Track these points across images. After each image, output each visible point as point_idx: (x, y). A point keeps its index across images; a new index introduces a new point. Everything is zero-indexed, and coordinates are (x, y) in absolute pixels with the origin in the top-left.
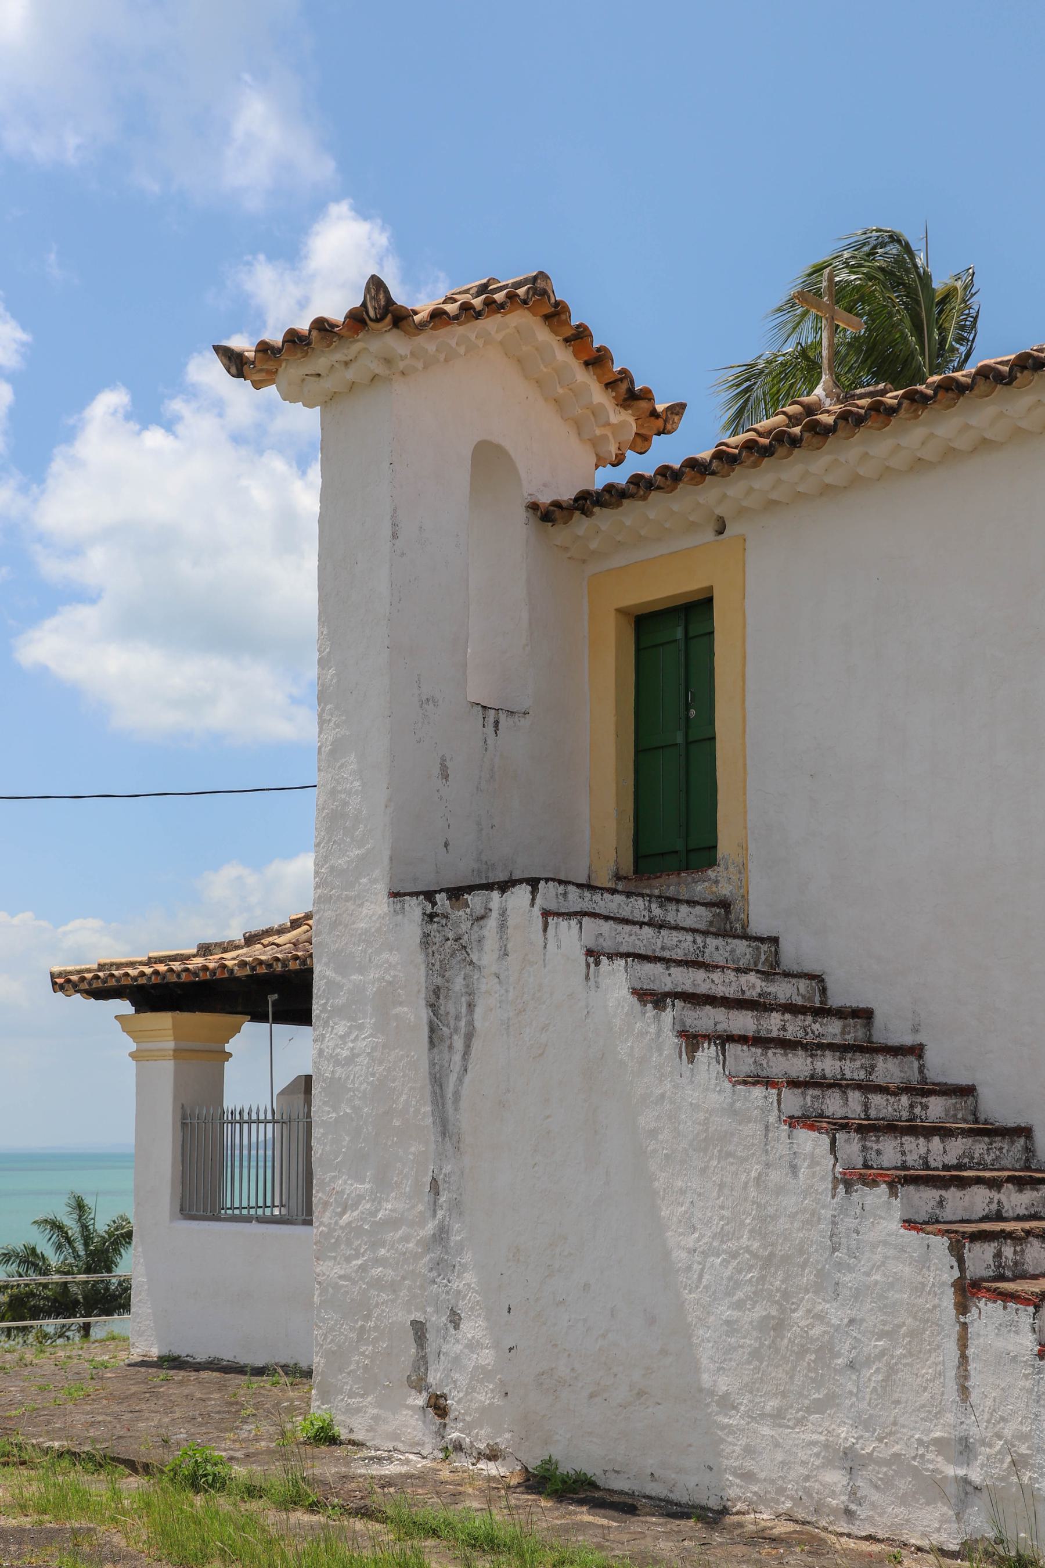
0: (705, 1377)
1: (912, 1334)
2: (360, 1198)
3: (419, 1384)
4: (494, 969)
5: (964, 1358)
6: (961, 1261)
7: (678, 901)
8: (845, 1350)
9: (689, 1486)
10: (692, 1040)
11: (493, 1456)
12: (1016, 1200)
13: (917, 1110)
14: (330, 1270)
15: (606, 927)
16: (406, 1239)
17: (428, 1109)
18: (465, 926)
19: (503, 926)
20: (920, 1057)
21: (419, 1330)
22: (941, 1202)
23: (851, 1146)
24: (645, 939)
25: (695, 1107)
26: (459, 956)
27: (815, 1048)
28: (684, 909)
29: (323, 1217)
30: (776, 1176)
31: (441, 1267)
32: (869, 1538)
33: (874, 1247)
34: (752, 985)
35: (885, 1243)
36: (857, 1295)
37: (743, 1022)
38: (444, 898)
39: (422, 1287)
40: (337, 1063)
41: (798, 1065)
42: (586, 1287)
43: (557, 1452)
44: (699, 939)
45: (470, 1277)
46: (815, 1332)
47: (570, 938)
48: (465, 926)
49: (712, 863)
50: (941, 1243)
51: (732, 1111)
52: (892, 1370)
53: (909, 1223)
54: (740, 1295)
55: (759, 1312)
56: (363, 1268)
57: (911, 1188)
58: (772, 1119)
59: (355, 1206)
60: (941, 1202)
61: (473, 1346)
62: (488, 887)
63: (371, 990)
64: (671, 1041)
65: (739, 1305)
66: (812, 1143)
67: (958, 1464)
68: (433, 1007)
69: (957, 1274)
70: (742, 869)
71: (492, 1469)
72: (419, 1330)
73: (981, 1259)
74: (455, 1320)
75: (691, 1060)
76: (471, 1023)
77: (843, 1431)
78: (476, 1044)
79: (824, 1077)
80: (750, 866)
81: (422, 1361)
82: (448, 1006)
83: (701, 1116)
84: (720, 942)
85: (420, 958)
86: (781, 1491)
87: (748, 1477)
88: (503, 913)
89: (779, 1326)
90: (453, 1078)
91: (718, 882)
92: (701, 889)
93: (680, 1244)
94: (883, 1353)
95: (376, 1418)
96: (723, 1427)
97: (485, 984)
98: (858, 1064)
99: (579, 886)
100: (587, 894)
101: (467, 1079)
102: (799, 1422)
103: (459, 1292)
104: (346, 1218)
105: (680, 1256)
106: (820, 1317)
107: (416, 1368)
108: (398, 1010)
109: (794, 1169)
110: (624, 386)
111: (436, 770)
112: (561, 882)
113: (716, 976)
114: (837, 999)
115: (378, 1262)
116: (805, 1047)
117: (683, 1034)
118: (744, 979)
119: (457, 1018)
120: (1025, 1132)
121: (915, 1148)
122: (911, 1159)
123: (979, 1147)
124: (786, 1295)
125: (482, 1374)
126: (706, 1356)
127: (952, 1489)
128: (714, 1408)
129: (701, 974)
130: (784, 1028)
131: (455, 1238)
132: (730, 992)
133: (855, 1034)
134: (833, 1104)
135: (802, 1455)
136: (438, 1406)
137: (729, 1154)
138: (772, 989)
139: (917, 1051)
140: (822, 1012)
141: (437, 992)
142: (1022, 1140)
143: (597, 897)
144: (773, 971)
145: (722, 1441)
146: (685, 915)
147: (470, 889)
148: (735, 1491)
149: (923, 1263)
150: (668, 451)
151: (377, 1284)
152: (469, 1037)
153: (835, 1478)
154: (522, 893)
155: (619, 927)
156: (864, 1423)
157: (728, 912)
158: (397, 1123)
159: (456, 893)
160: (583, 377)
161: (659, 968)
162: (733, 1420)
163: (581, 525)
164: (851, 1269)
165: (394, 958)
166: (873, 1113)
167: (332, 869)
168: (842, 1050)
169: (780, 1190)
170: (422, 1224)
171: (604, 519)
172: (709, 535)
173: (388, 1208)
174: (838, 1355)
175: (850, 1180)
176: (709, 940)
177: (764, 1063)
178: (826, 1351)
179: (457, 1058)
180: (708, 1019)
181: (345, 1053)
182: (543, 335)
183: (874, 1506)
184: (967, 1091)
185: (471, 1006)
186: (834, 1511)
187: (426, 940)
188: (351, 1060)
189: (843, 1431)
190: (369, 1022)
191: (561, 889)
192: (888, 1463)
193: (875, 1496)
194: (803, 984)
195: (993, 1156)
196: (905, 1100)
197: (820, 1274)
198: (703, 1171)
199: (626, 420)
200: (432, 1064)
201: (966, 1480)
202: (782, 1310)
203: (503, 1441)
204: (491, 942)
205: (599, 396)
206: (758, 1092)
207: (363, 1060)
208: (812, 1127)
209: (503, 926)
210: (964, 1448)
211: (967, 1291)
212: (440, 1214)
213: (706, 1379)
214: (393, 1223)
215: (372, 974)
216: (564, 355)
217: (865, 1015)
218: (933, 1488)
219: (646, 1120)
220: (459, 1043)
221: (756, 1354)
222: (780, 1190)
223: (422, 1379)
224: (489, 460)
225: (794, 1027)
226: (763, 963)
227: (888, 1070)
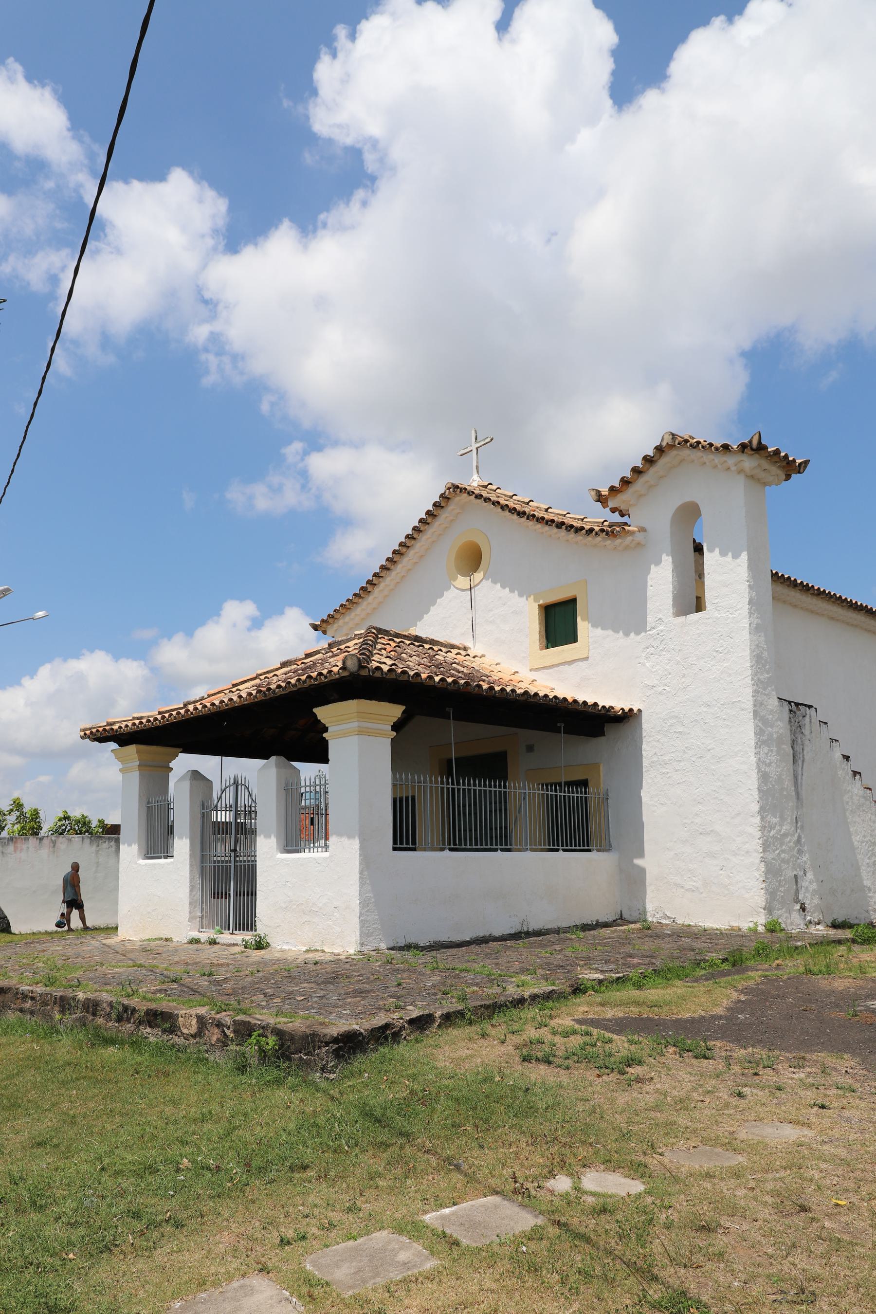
3: (797, 900)
11: (819, 924)
17: (793, 788)
31: (800, 852)
51: (864, 797)
56: (779, 854)
63: (775, 736)
65: (869, 858)
85: (789, 727)
93: (856, 839)
104: (772, 833)
108: (784, 746)
115: (783, 851)
136: (803, 909)
141: (793, 741)
152: (803, 761)
158: (785, 793)
159: (797, 704)
167: (759, 679)
173: (786, 828)
181: (768, 761)
187: (790, 721)
188: (770, 765)
204: (807, 726)
214: (785, 835)
215: (775, 730)
219: (846, 798)
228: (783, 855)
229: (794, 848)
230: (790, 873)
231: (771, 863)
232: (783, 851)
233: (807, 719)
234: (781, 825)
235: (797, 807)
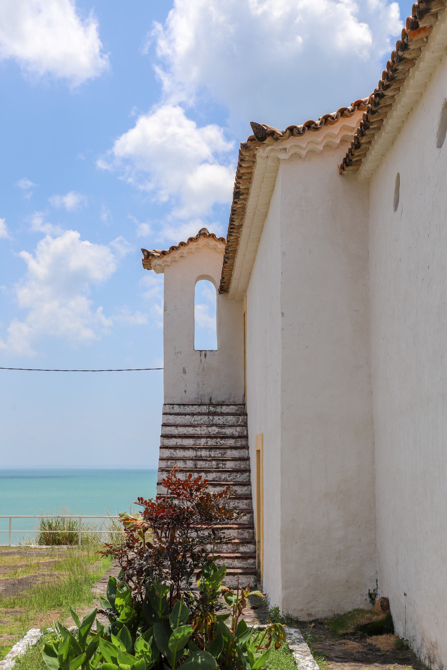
15: (171, 417)
20: (248, 449)
28: (224, 408)
44: (211, 417)
79: (201, 457)
98: (218, 452)
99: (178, 405)
100: (182, 407)
112: (171, 405)
113: (198, 429)
118: (210, 429)
129: (191, 429)
130: (207, 443)
138: (223, 431)
142: (248, 474)
143: (186, 407)
155: (176, 417)
161: (173, 428)
166: (199, 466)
176: (215, 417)
177: (175, 454)
191: (171, 406)
195: (231, 478)
196: (214, 463)
226: (241, 422)
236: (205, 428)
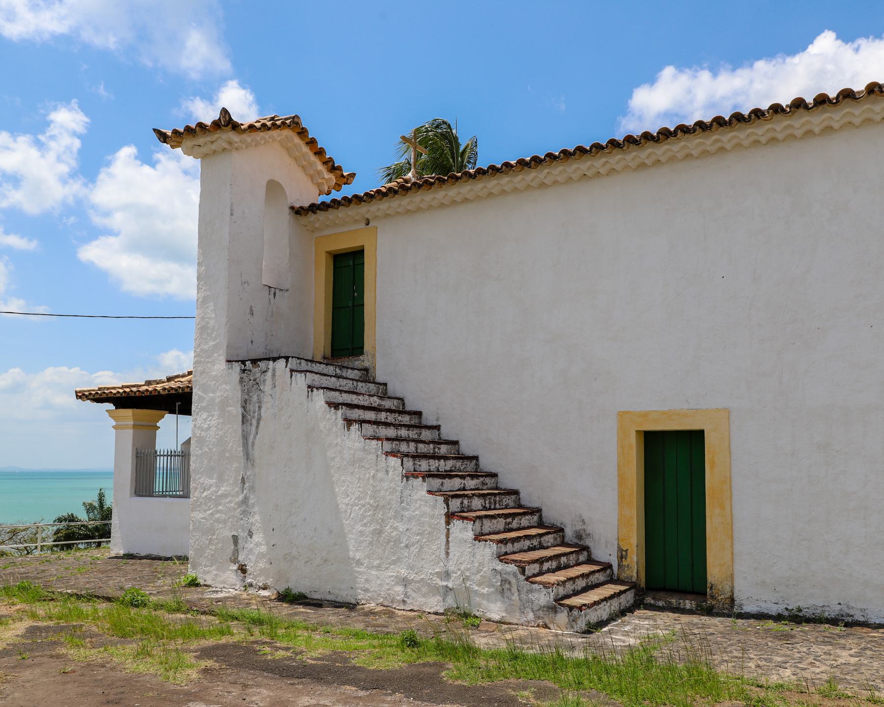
0: (351, 553)
1: (429, 533)
2: (211, 486)
3: (235, 560)
4: (270, 393)
5: (448, 541)
6: (448, 505)
7: (347, 368)
8: (405, 541)
9: (344, 595)
10: (349, 422)
11: (265, 588)
12: (471, 483)
13: (436, 450)
14: (198, 515)
15: (316, 377)
16: (230, 502)
18: (258, 375)
19: (274, 375)
20: (439, 430)
21: (235, 539)
22: (442, 484)
23: (409, 463)
24: (332, 382)
25: (349, 448)
26: (255, 387)
27: (397, 426)
28: (350, 371)
29: (195, 495)
30: (380, 475)
31: (245, 513)
32: (411, 610)
33: (416, 501)
34: (375, 401)
35: (420, 500)
36: (410, 520)
37: (370, 415)
38: (249, 364)
39: (237, 522)
40: (202, 430)
41: (391, 432)
42: (305, 519)
43: (291, 585)
45: (257, 517)
46: (393, 534)
47: (301, 381)
48: (258, 375)
49: (362, 353)
50: (441, 499)
51: (364, 450)
52: (422, 547)
53: (430, 492)
54: (365, 521)
55: (372, 527)
56: (212, 514)
57: (431, 479)
58: (379, 453)
59: (209, 489)
60: (442, 484)
61: (258, 545)
62: (268, 359)
63: (217, 400)
64: (341, 422)
65: (365, 525)
66: (394, 462)
67: (445, 581)
68: (244, 407)
69: (446, 510)
70: (374, 356)
71: (265, 593)
72: (235, 539)
73: (455, 504)
74: (251, 534)
75: (349, 429)
76: (259, 414)
77: (403, 571)
78: (262, 423)
80: (377, 355)
81: (236, 552)
82: (250, 407)
83: (352, 452)
84: (363, 384)
86: (379, 595)
87: (366, 590)
88: (274, 370)
89: (380, 532)
90: (252, 437)
91: (364, 361)
92: (357, 364)
93: (343, 502)
94: (418, 541)
95: (216, 575)
96: (357, 572)
97: (266, 399)
101: (258, 437)
102: (387, 569)
103: (252, 523)
105: (342, 507)
106: (396, 528)
107: (234, 554)
109: (387, 472)
110: (330, 164)
111: (248, 311)
112: (298, 358)
113: (361, 397)
114: (408, 408)
115: (218, 512)
116: (394, 425)
117: (345, 419)
118: (372, 399)
119: (254, 412)
120: (476, 458)
121: (434, 464)
122: (432, 468)
123: (459, 464)
124: (383, 520)
125: (262, 556)
126: (351, 545)
127: (441, 590)
128: (354, 565)
129: (354, 397)
131: (251, 501)
132: (366, 404)
133: (415, 421)
134: (404, 447)
135: (387, 581)
136: (243, 569)
137: (362, 467)
138: (383, 403)
139: (438, 428)
140: (401, 413)
141: (246, 401)
143: (314, 365)
144: (384, 396)
145: (357, 577)
146: (350, 373)
147: (260, 360)
148: (361, 596)
149: (434, 507)
150: (348, 191)
151: (218, 521)
152: (259, 420)
153: (399, 589)
154: (282, 362)
156: (411, 568)
157: (368, 373)
158: (227, 455)
159: (254, 362)
160: (313, 158)
161: (337, 393)
162: (362, 569)
163: (312, 217)
164: (407, 510)
165: (228, 387)
166: (419, 451)
168: (408, 427)
169: (381, 480)
170: (237, 496)
171: (321, 215)
172: (363, 225)
173: (223, 489)
174: (402, 543)
175: (408, 476)
178: (397, 541)
179: (254, 428)
180: (356, 414)
181: (206, 426)
182: (297, 140)
183: (413, 598)
184: (455, 443)
185: (260, 407)
186: (398, 601)
187: (241, 380)
189: (403, 571)
190: (216, 413)
191: (298, 361)
192: (419, 582)
193: (414, 595)
194: (395, 402)
196: (431, 446)
197: (396, 512)
198: (352, 473)
199: (331, 177)
200: (243, 431)
201: (447, 587)
202: (381, 526)
203: (269, 582)
204: (269, 381)
205: (320, 167)
206: (374, 442)
207: (214, 429)
208: (394, 456)
209: (274, 375)
210: (447, 575)
211: (450, 516)
212: (245, 492)
213: (351, 554)
214: (224, 496)
216: (305, 149)
217: (419, 414)
218: (435, 590)
219: (330, 454)
220: (254, 422)
221: (371, 543)
222: (381, 480)
223: (236, 558)
224: (274, 188)
225: (391, 418)
227: (426, 435)
228: (217, 516)
229: (235, 509)
230: (230, 534)
231: (200, 522)
232: (220, 512)
233: (269, 374)
234: (218, 487)
235: (246, 468)
236: (367, 397)
